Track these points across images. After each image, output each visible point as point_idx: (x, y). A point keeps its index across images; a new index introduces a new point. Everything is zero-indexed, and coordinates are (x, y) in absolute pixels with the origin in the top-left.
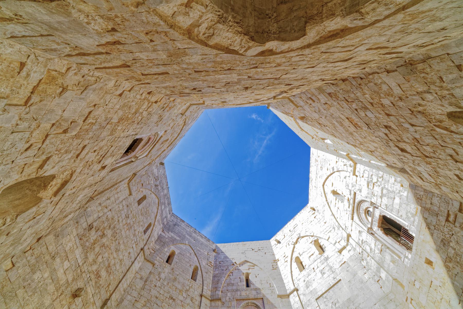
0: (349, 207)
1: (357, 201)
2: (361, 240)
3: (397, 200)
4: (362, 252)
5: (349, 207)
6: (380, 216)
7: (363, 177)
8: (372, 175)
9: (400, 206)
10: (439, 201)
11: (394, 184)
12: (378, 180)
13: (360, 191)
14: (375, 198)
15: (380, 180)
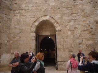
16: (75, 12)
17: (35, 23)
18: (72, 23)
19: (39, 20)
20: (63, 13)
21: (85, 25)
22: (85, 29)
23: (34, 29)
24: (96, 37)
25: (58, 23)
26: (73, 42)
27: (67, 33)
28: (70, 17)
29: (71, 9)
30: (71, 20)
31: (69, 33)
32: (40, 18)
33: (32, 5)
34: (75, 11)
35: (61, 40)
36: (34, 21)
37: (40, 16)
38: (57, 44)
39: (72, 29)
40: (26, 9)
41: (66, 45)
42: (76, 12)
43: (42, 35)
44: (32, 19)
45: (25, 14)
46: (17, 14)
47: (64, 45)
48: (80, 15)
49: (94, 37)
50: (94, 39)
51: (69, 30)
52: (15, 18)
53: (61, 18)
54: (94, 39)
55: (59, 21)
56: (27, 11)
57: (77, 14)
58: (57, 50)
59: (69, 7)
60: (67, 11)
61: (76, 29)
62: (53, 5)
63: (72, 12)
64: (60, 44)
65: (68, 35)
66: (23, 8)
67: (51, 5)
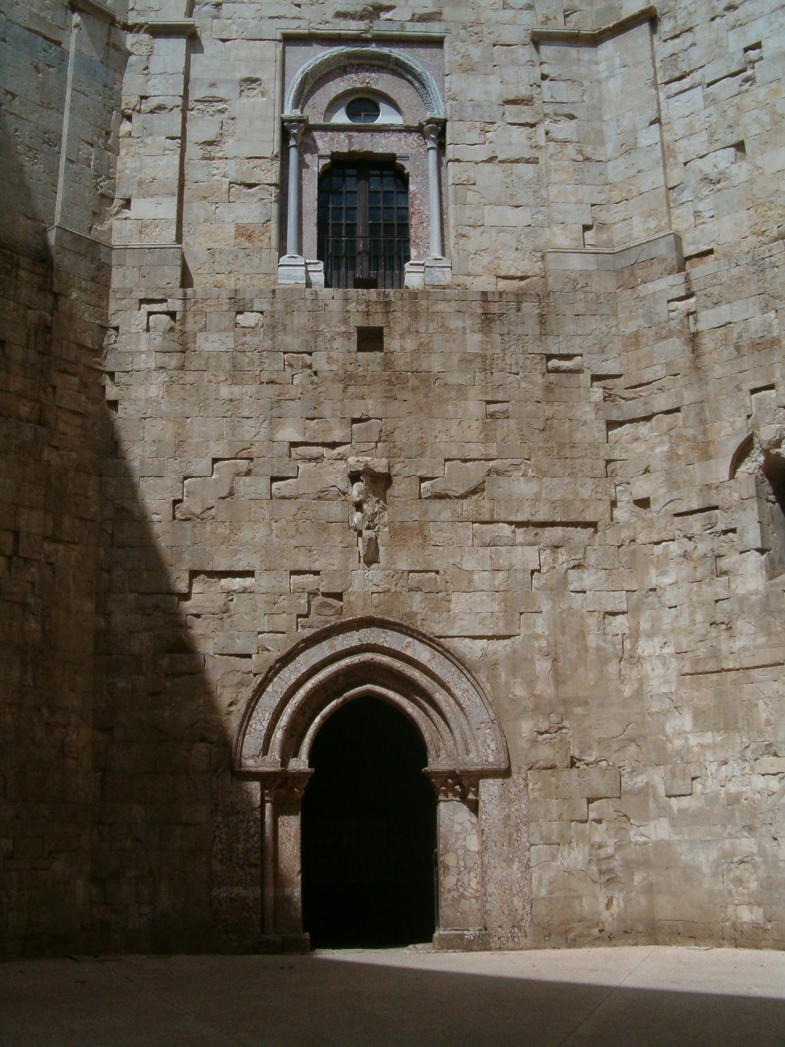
0: (340, 15)
1: (397, 52)
2: (220, 92)
3: (519, 217)
4: (160, 108)
5: (340, 15)
6: (393, 157)
7: (544, 77)
8: (572, 117)
9: (501, 229)
10: (597, 332)
11: (580, 202)
12: (566, 142)
13: (468, 69)
14: (474, 136)
15: (570, 150)
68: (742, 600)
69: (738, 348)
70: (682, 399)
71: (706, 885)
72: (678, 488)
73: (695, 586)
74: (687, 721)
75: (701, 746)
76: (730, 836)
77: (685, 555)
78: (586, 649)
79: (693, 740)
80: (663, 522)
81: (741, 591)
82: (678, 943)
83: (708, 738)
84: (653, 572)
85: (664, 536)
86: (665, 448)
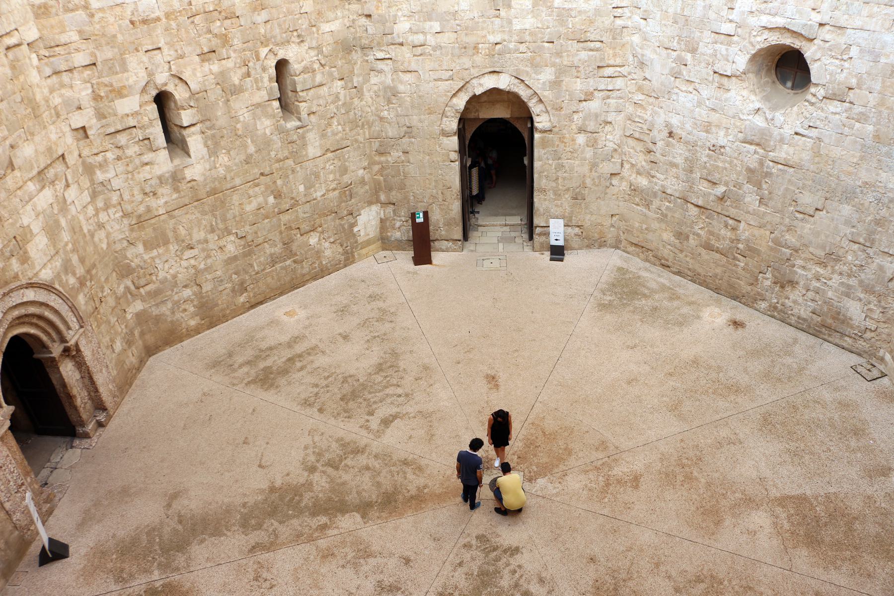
16: (611, 62)
17: (455, 100)
18: (594, 105)
19: (470, 90)
20: (565, 63)
21: (637, 119)
22: (637, 135)
23: (454, 125)
24: (658, 175)
25: (541, 101)
26: (591, 170)
27: (573, 140)
28: (591, 81)
29: (598, 45)
30: (592, 93)
31: (581, 139)
32: (475, 81)
33: (437, 27)
34: (615, 55)
35: (550, 162)
36: (450, 94)
37: (475, 72)
38: (536, 176)
39: (591, 126)
40: (417, 43)
41: (564, 179)
42: (618, 61)
43: (476, 119)
44: (443, 86)
45: (413, 66)
46: (380, 65)
47: (557, 179)
48: (630, 74)
49: (653, 172)
50: (653, 177)
51: (581, 130)
52: (374, 80)
53: (556, 84)
54: (653, 177)
55: (547, 94)
56: (419, 50)
57: (618, 69)
58: (535, 194)
59: (592, 38)
60: (584, 55)
61: (608, 128)
62: (527, 26)
63: (602, 59)
64: (547, 177)
65: (576, 147)
66: (401, 40)
67: (517, 26)
68: (160, 178)
69: (132, 22)
70: (96, 57)
71: (169, 319)
72: (106, 118)
73: (130, 176)
74: (140, 248)
75: (152, 258)
76: (177, 293)
77: (119, 158)
78: (85, 235)
79: (146, 257)
80: (99, 141)
81: (159, 173)
82: (160, 351)
83: (155, 253)
84: (98, 172)
85: (101, 149)
86: (90, 91)
